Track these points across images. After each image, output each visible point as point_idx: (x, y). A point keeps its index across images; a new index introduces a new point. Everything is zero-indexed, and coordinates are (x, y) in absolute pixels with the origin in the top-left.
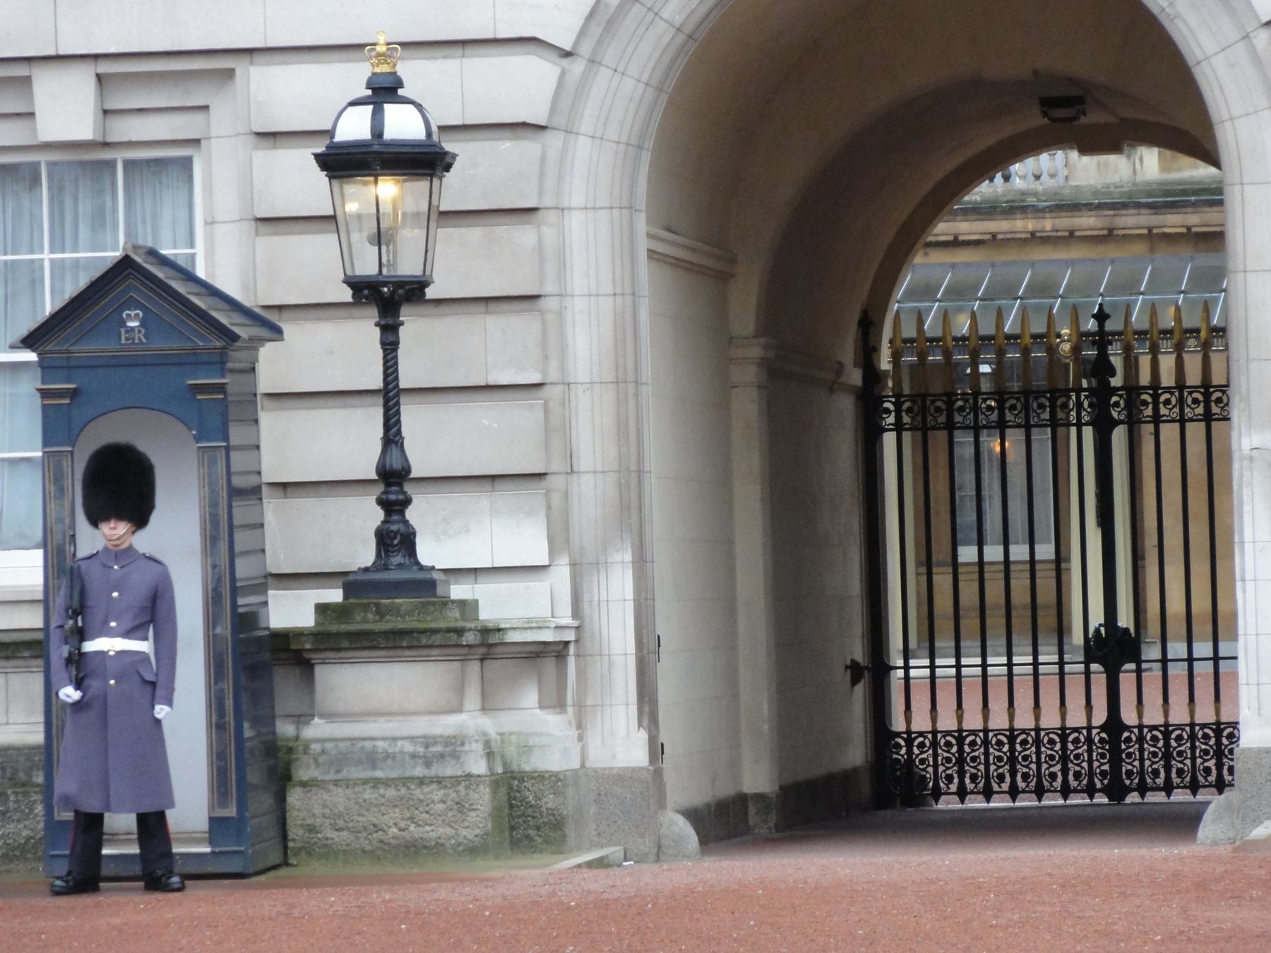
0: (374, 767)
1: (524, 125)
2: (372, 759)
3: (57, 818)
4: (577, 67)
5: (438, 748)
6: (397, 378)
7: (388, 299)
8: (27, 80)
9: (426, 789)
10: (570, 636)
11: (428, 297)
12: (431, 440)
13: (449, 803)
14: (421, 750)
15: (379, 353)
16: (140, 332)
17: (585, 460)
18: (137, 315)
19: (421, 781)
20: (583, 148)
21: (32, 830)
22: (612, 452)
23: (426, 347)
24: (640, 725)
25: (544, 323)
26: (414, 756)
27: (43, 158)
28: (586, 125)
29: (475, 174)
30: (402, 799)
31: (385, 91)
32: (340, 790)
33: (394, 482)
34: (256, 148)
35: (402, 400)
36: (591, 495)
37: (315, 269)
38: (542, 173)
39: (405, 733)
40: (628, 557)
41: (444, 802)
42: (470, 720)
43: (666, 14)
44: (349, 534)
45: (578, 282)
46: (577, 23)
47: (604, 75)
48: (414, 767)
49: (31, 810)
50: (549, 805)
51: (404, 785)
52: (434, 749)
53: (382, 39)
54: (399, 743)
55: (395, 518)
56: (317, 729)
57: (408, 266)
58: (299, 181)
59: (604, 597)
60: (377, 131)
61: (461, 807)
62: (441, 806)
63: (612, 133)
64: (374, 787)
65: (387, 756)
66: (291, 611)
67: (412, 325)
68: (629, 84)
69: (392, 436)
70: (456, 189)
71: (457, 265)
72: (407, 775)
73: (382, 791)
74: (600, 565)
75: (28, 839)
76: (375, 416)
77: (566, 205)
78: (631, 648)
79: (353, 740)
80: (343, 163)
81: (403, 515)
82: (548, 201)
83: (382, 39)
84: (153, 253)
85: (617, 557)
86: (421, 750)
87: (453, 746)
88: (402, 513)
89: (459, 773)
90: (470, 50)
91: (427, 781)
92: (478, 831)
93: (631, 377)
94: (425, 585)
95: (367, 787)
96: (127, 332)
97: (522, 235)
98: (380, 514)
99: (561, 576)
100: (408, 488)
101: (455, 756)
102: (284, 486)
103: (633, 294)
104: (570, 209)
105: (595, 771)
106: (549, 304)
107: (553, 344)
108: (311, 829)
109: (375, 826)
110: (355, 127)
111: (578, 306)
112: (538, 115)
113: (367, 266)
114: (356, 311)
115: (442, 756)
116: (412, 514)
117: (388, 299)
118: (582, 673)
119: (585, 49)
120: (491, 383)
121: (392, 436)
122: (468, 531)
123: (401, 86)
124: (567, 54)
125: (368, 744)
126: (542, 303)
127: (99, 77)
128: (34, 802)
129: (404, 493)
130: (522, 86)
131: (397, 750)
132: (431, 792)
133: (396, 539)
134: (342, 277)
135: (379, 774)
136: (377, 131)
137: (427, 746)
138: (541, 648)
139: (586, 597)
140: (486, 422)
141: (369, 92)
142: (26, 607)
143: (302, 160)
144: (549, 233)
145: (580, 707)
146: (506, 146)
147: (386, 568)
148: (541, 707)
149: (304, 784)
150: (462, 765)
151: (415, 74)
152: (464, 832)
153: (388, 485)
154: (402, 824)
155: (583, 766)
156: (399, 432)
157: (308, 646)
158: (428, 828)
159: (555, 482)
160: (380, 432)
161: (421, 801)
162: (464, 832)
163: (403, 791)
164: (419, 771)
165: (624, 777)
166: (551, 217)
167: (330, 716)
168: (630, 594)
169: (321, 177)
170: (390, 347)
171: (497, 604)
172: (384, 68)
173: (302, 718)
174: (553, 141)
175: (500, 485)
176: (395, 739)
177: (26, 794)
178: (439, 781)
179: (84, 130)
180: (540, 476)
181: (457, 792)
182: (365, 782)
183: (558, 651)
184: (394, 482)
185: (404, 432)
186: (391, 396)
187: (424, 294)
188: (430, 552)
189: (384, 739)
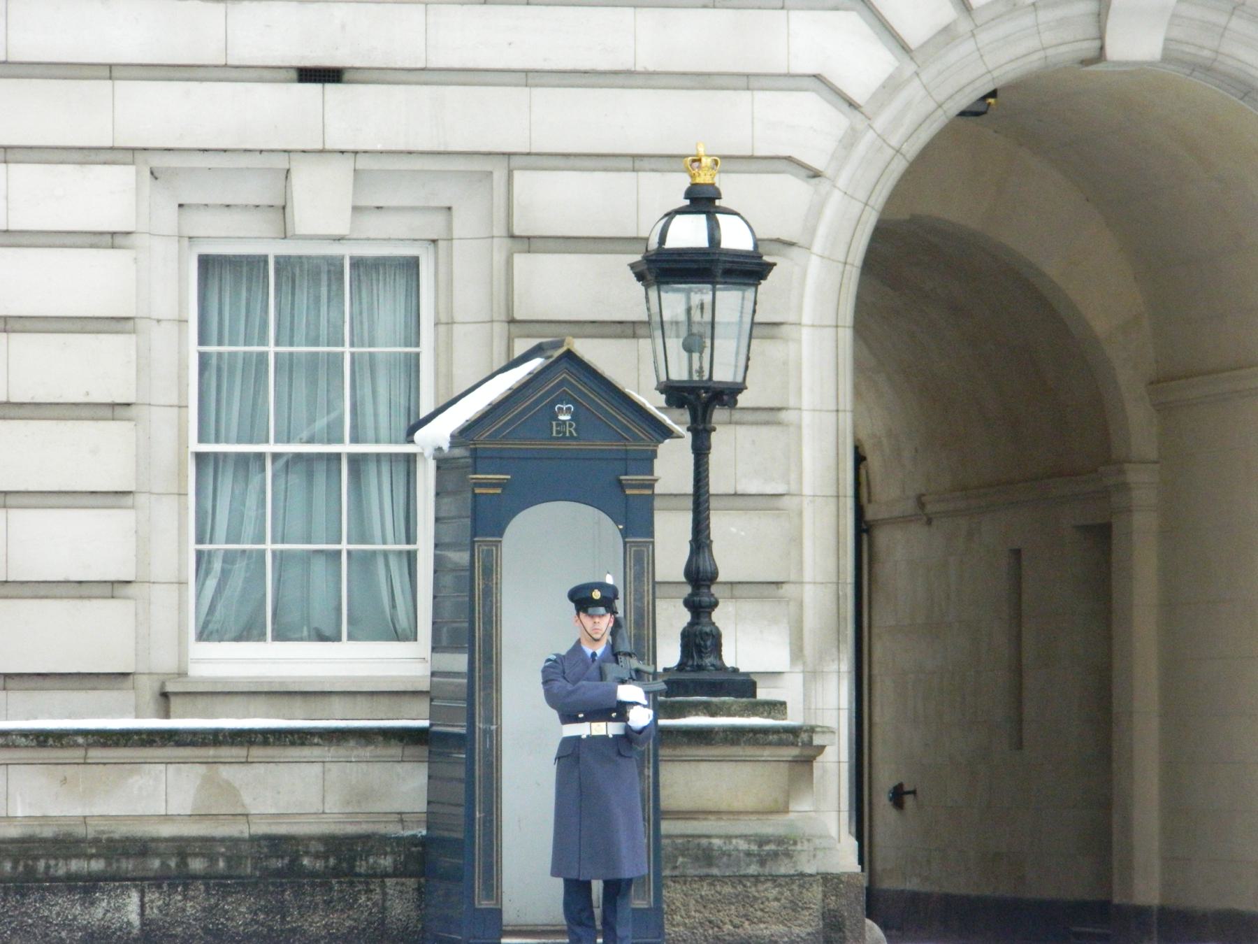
0: (710, 865)
3: (477, 906)
5: (771, 847)
9: (761, 887)
11: (740, 405)
13: (783, 901)
14: (754, 848)
15: (690, 458)
16: (571, 426)
18: (569, 409)
19: (757, 879)
21: (355, 920)
22: (831, 563)
26: (748, 854)
28: (817, 247)
30: (737, 896)
32: (678, 886)
39: (737, 832)
41: (777, 899)
45: (807, 400)
48: (748, 865)
49: (356, 900)
50: (831, 906)
51: (740, 882)
52: (767, 848)
53: (702, 151)
54: (734, 841)
57: (724, 374)
60: (714, 238)
61: (795, 906)
62: (776, 904)
64: (712, 884)
65: (724, 853)
72: (742, 873)
73: (718, 888)
75: (351, 929)
80: (664, 268)
86: (754, 848)
88: (710, 614)
89: (792, 872)
91: (762, 879)
92: (809, 930)
94: (742, 687)
95: (705, 884)
96: (558, 425)
98: (685, 617)
101: (788, 854)
109: (710, 922)
110: (689, 233)
111: (807, 418)
113: (679, 372)
115: (776, 854)
116: (719, 617)
125: (704, 841)
128: (359, 891)
131: (732, 847)
132: (766, 890)
133: (700, 641)
134: (655, 384)
135: (715, 871)
136: (714, 238)
137: (760, 845)
140: (733, 530)
141: (687, 202)
143: (621, 263)
147: (700, 668)
150: (795, 863)
152: (796, 930)
154: (737, 921)
156: (708, 536)
158: (762, 926)
160: (689, 537)
161: (756, 899)
162: (796, 930)
163: (740, 888)
164: (753, 869)
169: (639, 287)
176: (729, 837)
177: (351, 884)
178: (774, 879)
181: (791, 890)
182: (702, 878)
185: (712, 537)
187: (736, 402)
188: (731, 656)
189: (719, 837)
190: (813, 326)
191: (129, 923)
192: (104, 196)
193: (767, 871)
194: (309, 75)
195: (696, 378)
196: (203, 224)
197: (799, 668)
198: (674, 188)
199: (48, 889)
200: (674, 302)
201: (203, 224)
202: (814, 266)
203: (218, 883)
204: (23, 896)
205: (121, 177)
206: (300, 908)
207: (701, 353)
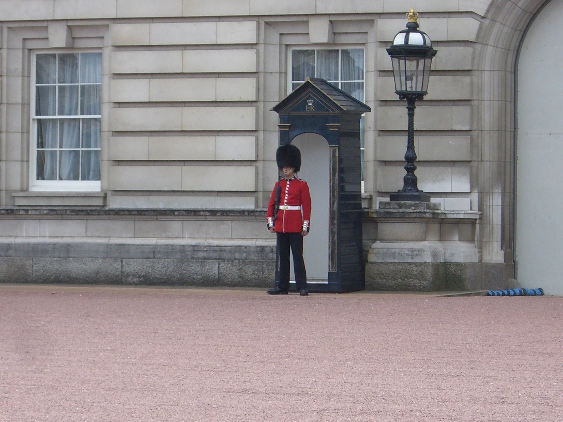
1: (468, 41)
2: (393, 255)
4: (487, 22)
6: (413, 126)
7: (411, 99)
8: (307, 22)
10: (477, 217)
12: (424, 148)
17: (486, 157)
19: (410, 264)
20: (490, 50)
24: (502, 249)
25: (472, 110)
27: (315, 48)
28: (491, 42)
29: (444, 58)
33: (411, 162)
34: (380, 47)
35: (415, 133)
36: (488, 169)
37: (390, 88)
38: (473, 58)
40: (500, 191)
43: (519, 5)
44: (396, 180)
45: (486, 96)
46: (486, 7)
47: (497, 25)
52: (415, 253)
55: (410, 173)
56: (378, 245)
59: (491, 204)
63: (500, 45)
67: (419, 110)
68: (506, 29)
69: (411, 146)
70: (436, 63)
71: (436, 88)
74: (491, 193)
76: (405, 139)
77: (483, 69)
78: (500, 222)
79: (389, 249)
81: (413, 173)
82: (475, 68)
83: (412, 11)
84: (323, 82)
85: (496, 191)
87: (420, 252)
90: (451, 15)
93: (504, 129)
97: (466, 79)
98: (405, 172)
99: (475, 196)
100: (415, 164)
102: (119, 162)
103: (506, 101)
104: (484, 70)
105: (485, 263)
106: (475, 103)
107: (475, 116)
108: (373, 278)
110: (399, 40)
112: (472, 38)
114: (401, 103)
117: (411, 99)
118: (482, 230)
119: (489, 16)
120: (453, 129)
121: (411, 146)
122: (443, 180)
123: (418, 27)
124: (483, 18)
125: (393, 250)
126: (472, 103)
127: (68, 26)
129: (413, 165)
130: (467, 28)
133: (411, 182)
135: (396, 261)
138: (456, 220)
139: (485, 204)
141: (407, 28)
142: (80, 198)
144: (475, 79)
145: (481, 241)
146: (461, 49)
148: (459, 241)
149: (371, 263)
151: (423, 23)
153: (408, 162)
155: (480, 261)
156: (413, 144)
157: (375, 216)
159: (474, 164)
163: (404, 266)
165: (494, 266)
166: (476, 73)
167: (382, 240)
168: (500, 203)
170: (411, 115)
172: (412, 20)
173: (374, 241)
174: (478, 47)
175: (456, 164)
178: (415, 264)
179: (324, 39)
180: (470, 161)
183: (473, 222)
184: (411, 162)
186: (411, 133)
190: (484, 70)
191: (214, 273)
192: (246, 32)
193: (413, 261)
195: (409, 89)
196: (288, 40)
197: (476, 191)
198: (403, 23)
199: (190, 262)
201: (288, 40)
202: (490, 50)
203: (244, 261)
204: (183, 263)
205: (251, 26)
206: (268, 270)
207: (411, 80)
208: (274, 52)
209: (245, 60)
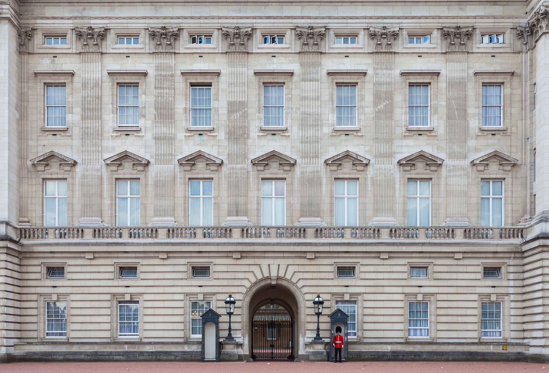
7: (230, 314)
12: (233, 326)
23: (233, 318)
31: (230, 296)
33: (230, 329)
42: (235, 350)
58: (223, 304)
66: (221, 340)
67: (232, 317)
69: (230, 326)
71: (236, 311)
94: (233, 338)
110: (228, 299)
117: (230, 314)
121: (230, 326)
133: (230, 334)
170: (230, 318)
171: (238, 340)
173: (223, 349)
184: (230, 329)
194: (199, 286)
196: (191, 299)
198: (228, 295)
200: (228, 305)
208: (188, 302)
209: (181, 304)
